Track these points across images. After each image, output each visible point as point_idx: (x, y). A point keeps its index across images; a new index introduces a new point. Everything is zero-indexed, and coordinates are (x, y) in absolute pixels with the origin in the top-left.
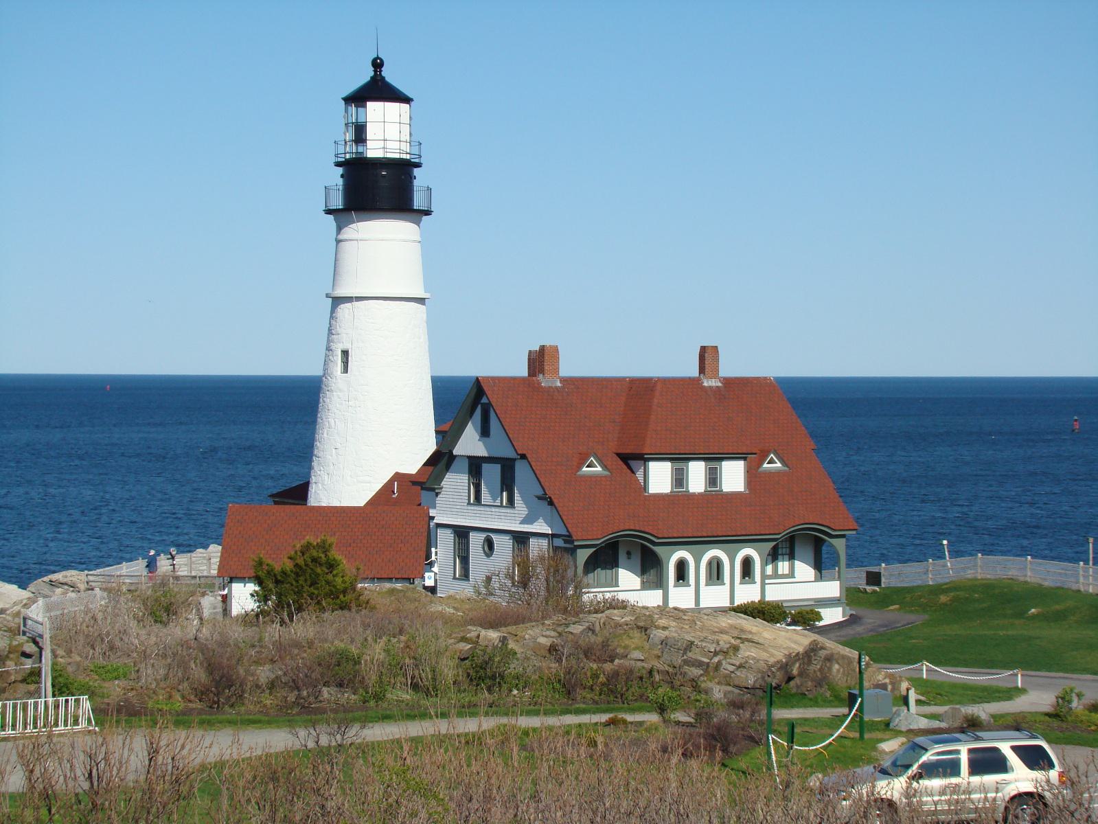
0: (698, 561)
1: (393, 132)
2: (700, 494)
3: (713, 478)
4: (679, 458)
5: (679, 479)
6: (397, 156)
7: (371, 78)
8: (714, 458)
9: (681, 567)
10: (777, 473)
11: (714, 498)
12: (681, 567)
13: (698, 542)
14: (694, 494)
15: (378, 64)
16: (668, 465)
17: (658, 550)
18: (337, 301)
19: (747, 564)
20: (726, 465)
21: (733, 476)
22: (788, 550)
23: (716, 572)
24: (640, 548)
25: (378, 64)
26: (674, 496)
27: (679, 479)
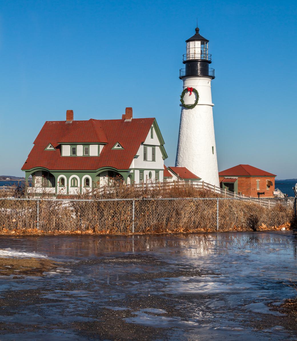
1: (192, 51)
2: (81, 157)
3: (87, 151)
4: (73, 144)
5: (74, 151)
7: (195, 34)
8: (87, 144)
11: (86, 159)
12: (62, 180)
15: (197, 30)
16: (69, 146)
17: (54, 174)
19: (87, 180)
20: (91, 146)
21: (94, 151)
24: (41, 173)
25: (197, 30)
26: (84, 157)
27: (74, 151)
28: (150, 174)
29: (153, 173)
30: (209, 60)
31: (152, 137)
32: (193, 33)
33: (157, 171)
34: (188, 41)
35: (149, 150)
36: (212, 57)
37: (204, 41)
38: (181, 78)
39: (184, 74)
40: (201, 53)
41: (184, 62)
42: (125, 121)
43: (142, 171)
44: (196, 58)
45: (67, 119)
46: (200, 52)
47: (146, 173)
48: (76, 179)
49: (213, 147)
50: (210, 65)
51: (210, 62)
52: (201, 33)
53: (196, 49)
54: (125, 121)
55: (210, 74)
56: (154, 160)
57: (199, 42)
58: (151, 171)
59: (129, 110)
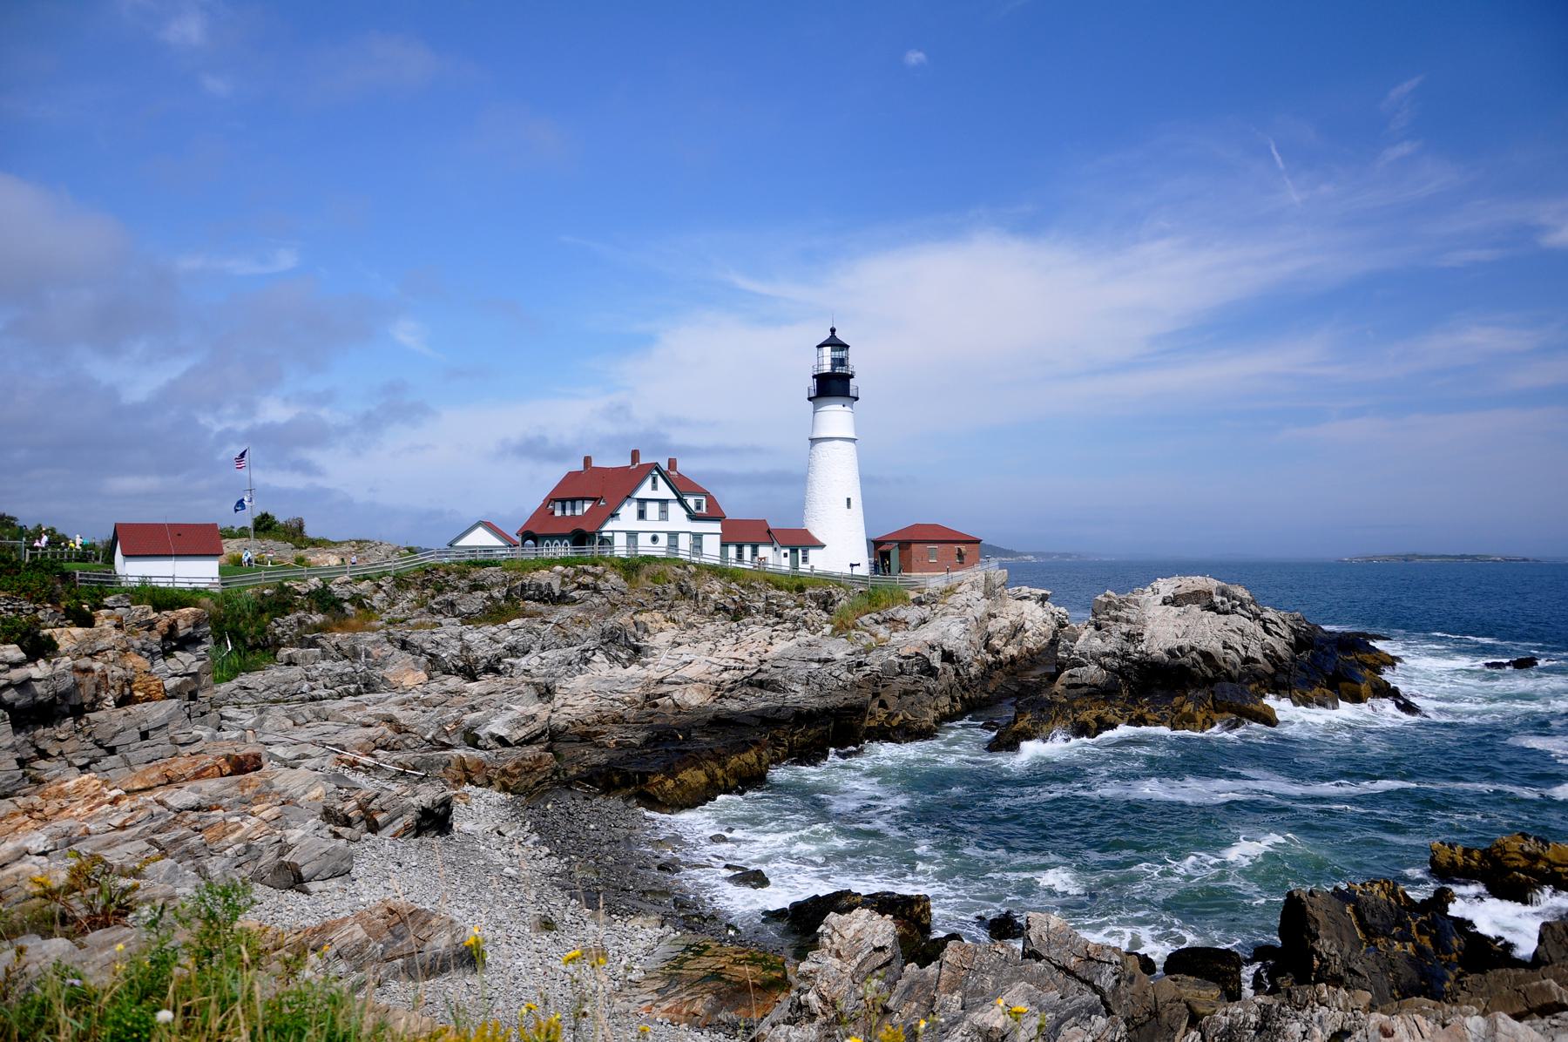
15: (833, 330)
18: (814, 441)
25: (833, 330)
28: (654, 539)
29: (663, 539)
31: (655, 487)
33: (673, 536)
43: (632, 535)
59: (635, 455)
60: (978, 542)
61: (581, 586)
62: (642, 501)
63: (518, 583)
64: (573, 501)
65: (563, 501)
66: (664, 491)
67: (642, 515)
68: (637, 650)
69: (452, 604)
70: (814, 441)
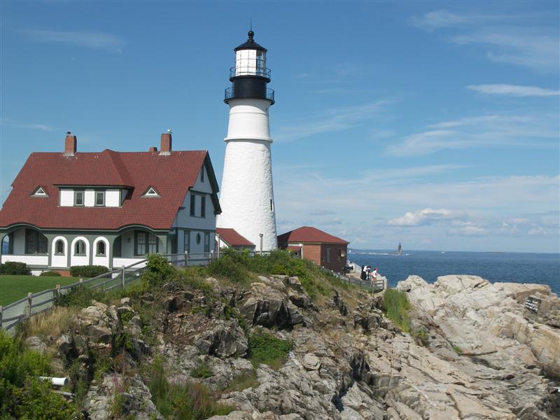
0: (69, 243)
1: (244, 63)
2: (91, 208)
3: (100, 200)
5: (79, 200)
6: (246, 74)
9: (60, 244)
10: (153, 198)
12: (60, 244)
13: (71, 232)
14: (87, 208)
15: (251, 35)
19: (101, 247)
22: (155, 242)
23: (80, 249)
25: (251, 35)
28: (199, 237)
30: (267, 77)
31: (202, 180)
32: (246, 39)
34: (237, 49)
35: (198, 199)
36: (271, 74)
37: (261, 50)
38: (227, 101)
39: (230, 96)
40: (257, 67)
41: (232, 79)
42: (160, 154)
43: (187, 231)
44: (250, 74)
45: (66, 149)
46: (255, 65)
47: (193, 235)
48: (84, 245)
49: (271, 201)
50: (268, 85)
51: (268, 81)
52: (255, 39)
53: (246, 63)
54: (160, 154)
55: (268, 96)
56: (203, 215)
57: (254, 52)
58: (200, 233)
60: (343, 246)
61: (298, 302)
62: (194, 194)
63: (250, 301)
64: (100, 189)
65: (79, 188)
66: (205, 187)
67: (192, 213)
68: (372, 381)
69: (231, 338)
70: (228, 141)
